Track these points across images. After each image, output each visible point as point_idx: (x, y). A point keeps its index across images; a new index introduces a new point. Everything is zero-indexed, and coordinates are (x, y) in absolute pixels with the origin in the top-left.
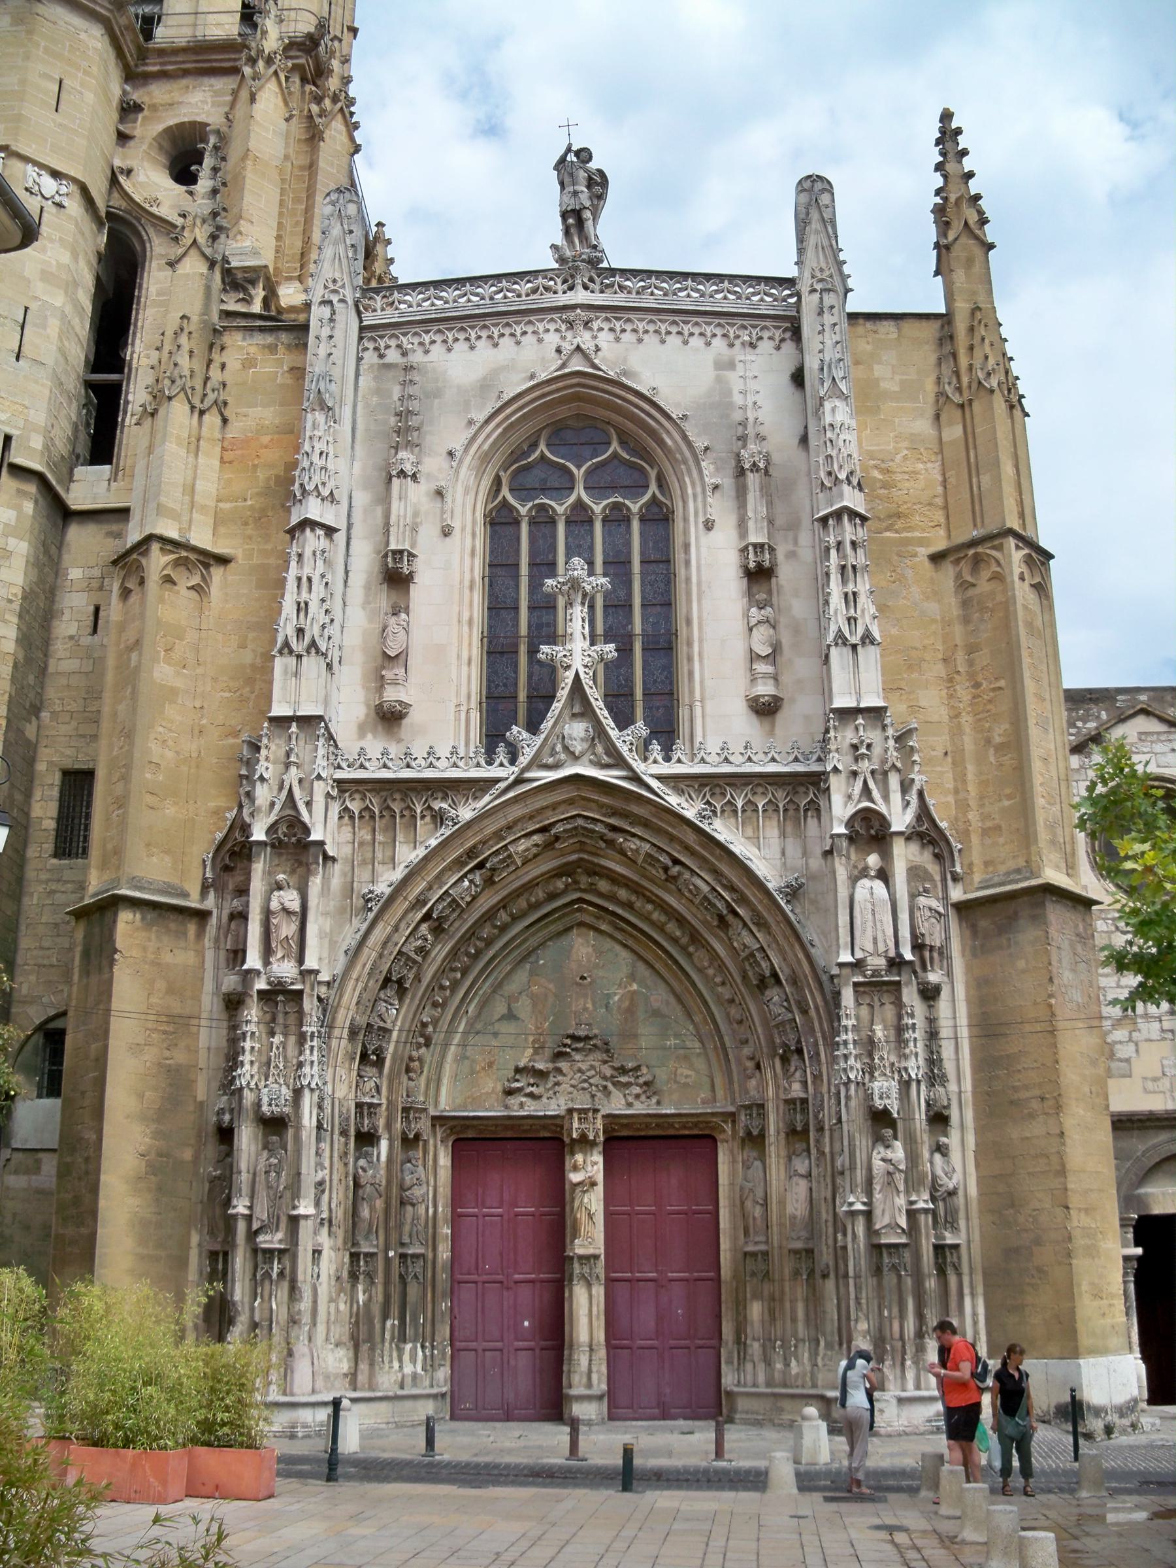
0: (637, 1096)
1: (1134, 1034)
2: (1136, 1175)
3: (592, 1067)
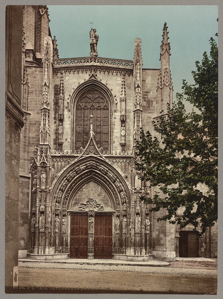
0: (100, 209)
3: (93, 204)
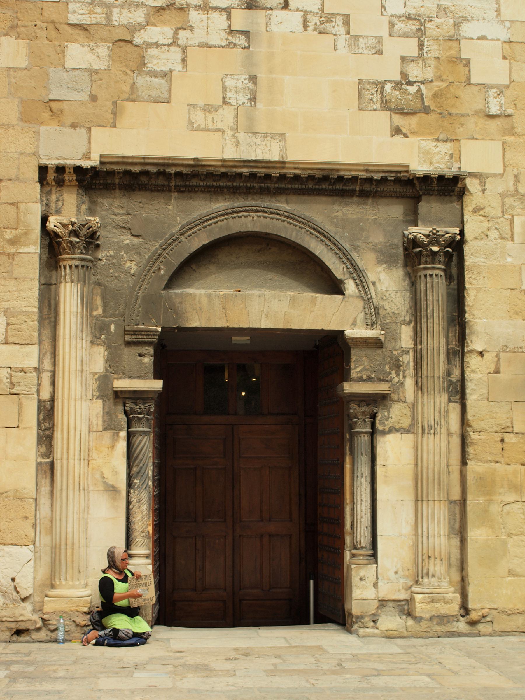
1: (181, 33)
2: (167, 264)
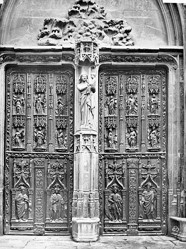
0: (121, 39)
